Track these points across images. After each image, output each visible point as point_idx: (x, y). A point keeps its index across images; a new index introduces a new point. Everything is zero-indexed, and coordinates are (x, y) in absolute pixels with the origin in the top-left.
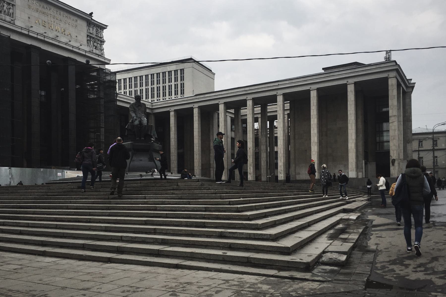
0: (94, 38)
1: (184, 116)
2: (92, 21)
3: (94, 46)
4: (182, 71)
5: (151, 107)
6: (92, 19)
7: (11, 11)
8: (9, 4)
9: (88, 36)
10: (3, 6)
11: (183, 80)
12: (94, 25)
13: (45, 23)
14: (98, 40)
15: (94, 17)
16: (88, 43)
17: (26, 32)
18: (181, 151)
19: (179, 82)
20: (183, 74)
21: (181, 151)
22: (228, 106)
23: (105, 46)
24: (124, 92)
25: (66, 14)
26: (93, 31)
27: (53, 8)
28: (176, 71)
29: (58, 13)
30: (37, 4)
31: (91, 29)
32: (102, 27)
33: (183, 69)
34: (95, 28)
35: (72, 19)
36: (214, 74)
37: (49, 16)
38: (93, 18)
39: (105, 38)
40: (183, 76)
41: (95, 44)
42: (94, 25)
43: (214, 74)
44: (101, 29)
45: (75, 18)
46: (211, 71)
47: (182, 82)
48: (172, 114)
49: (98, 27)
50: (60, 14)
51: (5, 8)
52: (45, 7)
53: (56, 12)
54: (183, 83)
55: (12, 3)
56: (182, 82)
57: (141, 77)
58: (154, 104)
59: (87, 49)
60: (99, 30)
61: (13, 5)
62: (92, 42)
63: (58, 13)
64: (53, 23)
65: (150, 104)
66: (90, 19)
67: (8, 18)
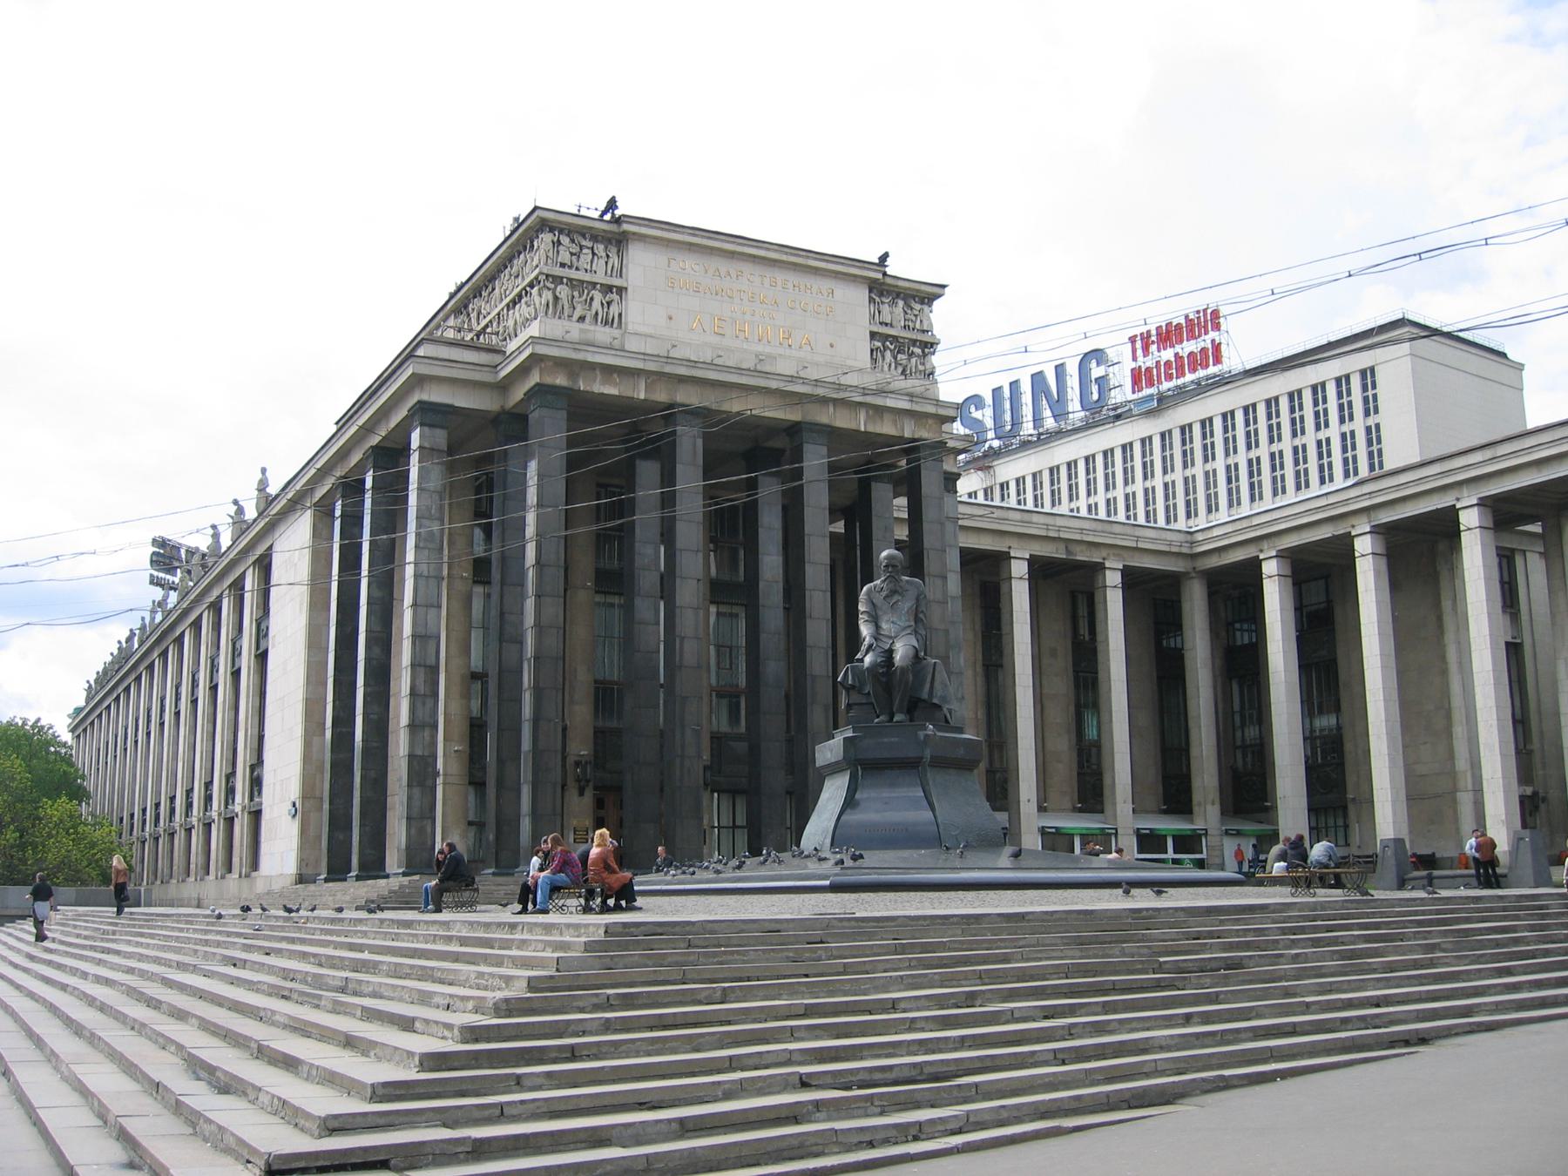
0: (895, 338)
1: (1321, 574)
2: (888, 281)
3: (897, 364)
4: (1368, 375)
5: (1184, 550)
6: (885, 274)
7: (614, 310)
8: (608, 289)
9: (873, 335)
11: (1376, 411)
14: (914, 342)
15: (893, 268)
16: (874, 360)
18: (1326, 722)
19: (1358, 425)
20: (1374, 387)
21: (1326, 722)
22: (1506, 513)
23: (936, 360)
24: (1089, 507)
25: (793, 278)
26: (894, 312)
27: (747, 268)
28: (1342, 382)
30: (696, 268)
31: (886, 309)
32: (924, 295)
33: (1372, 369)
34: (901, 303)
35: (814, 290)
36: (1520, 367)
38: (889, 271)
39: (938, 331)
40: (1375, 396)
43: (1520, 367)
44: (922, 303)
45: (826, 284)
46: (1504, 355)
47: (1371, 421)
48: (1270, 568)
50: (773, 285)
51: (596, 305)
52: (723, 271)
53: (757, 280)
54: (1378, 426)
55: (617, 282)
56: (1371, 421)
57: (1206, 423)
58: (1200, 537)
59: (869, 380)
60: (918, 307)
61: (621, 290)
62: (888, 354)
63: (766, 281)
64: (748, 317)
65: (1181, 537)
66: (880, 276)
67: (603, 334)
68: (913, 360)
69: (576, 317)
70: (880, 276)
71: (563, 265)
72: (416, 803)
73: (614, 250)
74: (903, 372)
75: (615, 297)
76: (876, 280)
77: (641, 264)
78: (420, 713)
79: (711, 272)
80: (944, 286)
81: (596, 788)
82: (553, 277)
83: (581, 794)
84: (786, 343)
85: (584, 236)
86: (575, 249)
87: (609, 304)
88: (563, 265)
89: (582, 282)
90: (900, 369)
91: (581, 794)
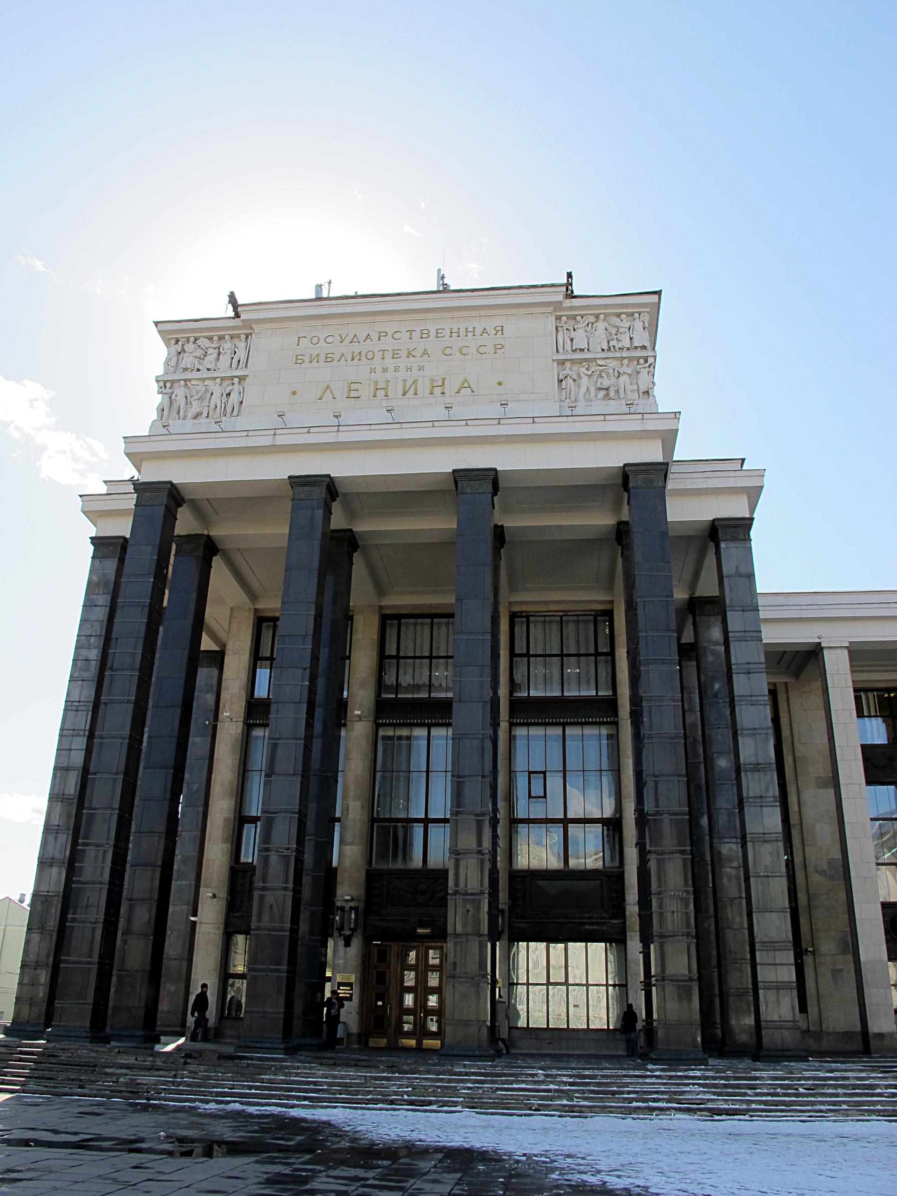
6: (570, 295)
7: (234, 398)
10: (212, 394)
12: (597, 317)
13: (353, 386)
17: (266, 441)
29: (416, 335)
30: (329, 340)
35: (478, 331)
37: (377, 360)
41: (606, 383)
42: (597, 317)
45: (490, 324)
49: (619, 315)
51: (216, 399)
52: (362, 337)
61: (242, 379)
62: (585, 379)
63: (416, 335)
68: (624, 379)
69: (192, 412)
70: (560, 298)
71: (185, 369)
72: (34, 948)
73: (241, 345)
74: (607, 397)
75: (236, 386)
76: (557, 305)
77: (268, 347)
78: (50, 848)
79: (349, 339)
80: (658, 293)
81: (367, 940)
82: (173, 382)
83: (347, 944)
84: (438, 390)
85: (210, 339)
86: (199, 353)
87: (229, 395)
88: (185, 369)
89: (203, 380)
90: (602, 394)
91: (347, 944)
